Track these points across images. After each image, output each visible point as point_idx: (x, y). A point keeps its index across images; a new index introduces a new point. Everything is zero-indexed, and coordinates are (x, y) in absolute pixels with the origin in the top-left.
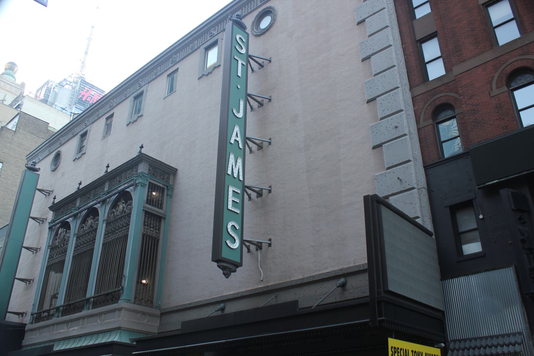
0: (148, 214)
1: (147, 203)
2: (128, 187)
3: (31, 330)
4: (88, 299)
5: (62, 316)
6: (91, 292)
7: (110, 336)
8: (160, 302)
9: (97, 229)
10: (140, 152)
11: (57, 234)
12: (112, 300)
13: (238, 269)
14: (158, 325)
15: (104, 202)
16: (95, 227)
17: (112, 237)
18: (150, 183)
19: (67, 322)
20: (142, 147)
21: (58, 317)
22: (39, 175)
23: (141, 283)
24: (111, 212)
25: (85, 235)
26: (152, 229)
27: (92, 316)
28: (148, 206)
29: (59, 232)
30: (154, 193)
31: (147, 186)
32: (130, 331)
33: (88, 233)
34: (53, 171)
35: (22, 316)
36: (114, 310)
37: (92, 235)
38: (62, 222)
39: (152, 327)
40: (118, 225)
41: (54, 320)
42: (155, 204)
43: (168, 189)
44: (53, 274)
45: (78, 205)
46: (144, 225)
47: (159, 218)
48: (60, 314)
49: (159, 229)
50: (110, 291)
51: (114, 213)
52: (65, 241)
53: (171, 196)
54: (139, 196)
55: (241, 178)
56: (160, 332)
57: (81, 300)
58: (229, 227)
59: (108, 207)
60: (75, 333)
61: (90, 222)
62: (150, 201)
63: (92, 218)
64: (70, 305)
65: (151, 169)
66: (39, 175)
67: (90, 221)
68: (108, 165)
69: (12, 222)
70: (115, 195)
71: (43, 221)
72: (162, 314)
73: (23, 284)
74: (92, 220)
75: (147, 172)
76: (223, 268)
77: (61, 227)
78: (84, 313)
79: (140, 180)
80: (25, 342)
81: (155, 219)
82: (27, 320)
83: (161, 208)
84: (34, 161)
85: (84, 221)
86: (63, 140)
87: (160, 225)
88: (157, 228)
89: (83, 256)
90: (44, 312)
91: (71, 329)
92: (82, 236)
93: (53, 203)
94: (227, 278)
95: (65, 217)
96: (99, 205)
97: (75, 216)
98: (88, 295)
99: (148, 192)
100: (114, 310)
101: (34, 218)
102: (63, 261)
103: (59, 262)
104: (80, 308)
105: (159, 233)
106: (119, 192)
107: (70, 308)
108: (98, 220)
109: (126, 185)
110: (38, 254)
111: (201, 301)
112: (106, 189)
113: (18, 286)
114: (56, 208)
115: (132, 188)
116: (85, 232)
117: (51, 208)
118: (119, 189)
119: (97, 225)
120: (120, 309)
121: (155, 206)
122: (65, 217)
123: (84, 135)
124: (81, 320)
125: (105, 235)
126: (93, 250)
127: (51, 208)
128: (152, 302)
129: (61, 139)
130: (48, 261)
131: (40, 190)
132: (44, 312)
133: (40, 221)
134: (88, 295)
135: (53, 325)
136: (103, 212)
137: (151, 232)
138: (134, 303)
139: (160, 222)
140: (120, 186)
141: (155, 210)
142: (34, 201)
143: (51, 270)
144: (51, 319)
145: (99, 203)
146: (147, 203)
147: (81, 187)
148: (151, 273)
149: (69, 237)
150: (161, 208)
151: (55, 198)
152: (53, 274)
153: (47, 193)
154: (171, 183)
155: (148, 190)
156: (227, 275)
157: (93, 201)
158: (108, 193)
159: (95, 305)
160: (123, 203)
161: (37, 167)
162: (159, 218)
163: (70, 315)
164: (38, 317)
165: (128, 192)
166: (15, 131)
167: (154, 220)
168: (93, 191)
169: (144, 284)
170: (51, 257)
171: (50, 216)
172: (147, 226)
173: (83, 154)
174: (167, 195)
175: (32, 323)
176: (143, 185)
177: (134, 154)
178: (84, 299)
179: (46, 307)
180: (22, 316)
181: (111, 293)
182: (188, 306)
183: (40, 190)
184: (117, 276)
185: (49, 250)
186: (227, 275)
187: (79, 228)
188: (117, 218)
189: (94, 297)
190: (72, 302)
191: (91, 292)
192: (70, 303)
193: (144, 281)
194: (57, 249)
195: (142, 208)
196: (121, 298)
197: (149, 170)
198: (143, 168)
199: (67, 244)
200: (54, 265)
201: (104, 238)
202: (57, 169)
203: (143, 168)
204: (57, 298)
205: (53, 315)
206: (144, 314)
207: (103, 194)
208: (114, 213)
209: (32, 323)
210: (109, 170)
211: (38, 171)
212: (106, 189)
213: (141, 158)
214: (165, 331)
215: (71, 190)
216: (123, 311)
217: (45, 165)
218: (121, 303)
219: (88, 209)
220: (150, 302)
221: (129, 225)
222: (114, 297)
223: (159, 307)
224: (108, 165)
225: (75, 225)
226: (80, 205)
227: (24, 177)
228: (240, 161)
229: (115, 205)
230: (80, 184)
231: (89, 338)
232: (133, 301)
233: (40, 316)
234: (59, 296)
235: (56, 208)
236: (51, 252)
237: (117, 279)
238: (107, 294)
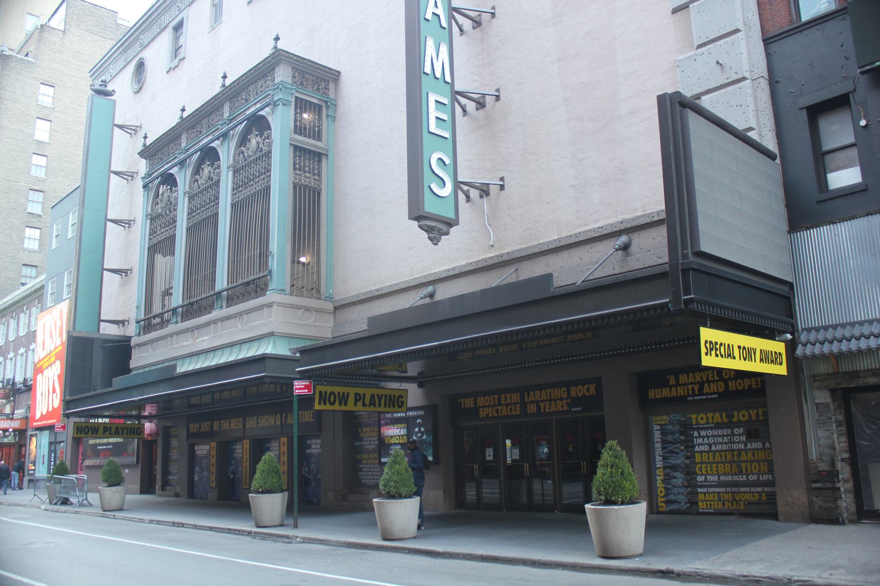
0: (297, 149)
1: (295, 132)
3: (140, 345)
4: (220, 293)
6: (222, 282)
8: (331, 291)
9: (219, 181)
10: (276, 47)
11: (157, 195)
12: (256, 292)
13: (453, 230)
14: (332, 326)
15: (225, 136)
16: (215, 178)
17: (245, 193)
18: (296, 98)
20: (277, 39)
21: (177, 322)
22: (115, 101)
23: (299, 262)
24: (239, 153)
25: (201, 192)
26: (308, 175)
27: (228, 318)
28: (297, 137)
29: (161, 192)
30: (305, 116)
31: (293, 104)
33: (206, 189)
34: (137, 92)
35: (124, 325)
36: (261, 308)
37: (213, 193)
38: (162, 175)
39: (323, 329)
40: (253, 172)
41: (171, 328)
42: (310, 133)
43: (328, 107)
44: (159, 258)
45: (183, 145)
46: (295, 169)
47: (318, 156)
48: (179, 319)
49: (319, 175)
50: (251, 278)
51: (243, 152)
52: (172, 206)
53: (334, 118)
54: (281, 122)
55: (448, 79)
56: (336, 335)
57: (208, 294)
58: (434, 162)
59: (233, 144)
60: (205, 346)
61: (206, 171)
62: (299, 129)
63: (209, 165)
64: (192, 304)
65: (297, 74)
66: (115, 101)
67: (206, 170)
68: (225, 74)
69: (85, 181)
70: (241, 123)
71: (132, 177)
72: (336, 308)
73: (116, 277)
74: (210, 168)
75: (289, 80)
76: (428, 230)
77: (163, 183)
78: (215, 314)
79: (280, 96)
80: (133, 364)
81: (310, 158)
82: (131, 330)
83: (319, 139)
84: (103, 78)
85: (197, 171)
86: (145, 38)
87: (320, 167)
88: (316, 172)
89: (203, 227)
90: (154, 317)
91: (198, 340)
92: (196, 195)
93: (145, 145)
94: (436, 244)
95: (166, 167)
96: (217, 142)
97: (182, 163)
98: (218, 287)
99: (296, 114)
100: (261, 308)
101: (117, 173)
102: (173, 237)
103: (166, 239)
105: (320, 180)
106: (248, 119)
107: (193, 309)
108: (219, 167)
109: (258, 106)
110: (133, 228)
111: (396, 285)
112: (226, 115)
113: (110, 281)
114: (150, 152)
115: (267, 109)
116: (201, 188)
117: (142, 154)
118: (248, 112)
119: (219, 175)
120: (270, 305)
121: (310, 137)
122: (166, 167)
123: (178, 27)
126: (216, 215)
127: (142, 154)
128: (319, 291)
129: (142, 37)
130: (150, 239)
131: (120, 127)
132: (154, 317)
133: (127, 176)
134: (218, 287)
136: (227, 153)
137: (307, 180)
138: (291, 294)
139: (320, 161)
140: (249, 108)
141: (309, 143)
142: (114, 145)
143: (155, 252)
144: (167, 326)
145: (218, 139)
146: (295, 132)
147: (185, 114)
148: (313, 245)
149: (176, 198)
150: (319, 139)
151: (145, 137)
152: (159, 258)
153: (131, 130)
154: (332, 96)
155: (295, 110)
156: (435, 241)
158: (231, 121)
159: (231, 300)
160: (257, 135)
161: (110, 88)
162: (318, 156)
164: (147, 326)
165: (263, 117)
166: (64, 32)
167: (309, 160)
168: (206, 120)
169: (303, 264)
170: (152, 233)
171: (142, 166)
172: (300, 170)
173: (181, 60)
174: (328, 116)
175: (139, 335)
176: (286, 104)
177: (266, 51)
178: (212, 293)
179: (157, 309)
180: (124, 325)
181: (253, 280)
182: (377, 294)
183: (120, 127)
184: (260, 254)
185: (149, 221)
186: (435, 241)
187: (190, 182)
188: (249, 160)
189: (227, 290)
190: (195, 299)
191: (222, 282)
192: (192, 300)
193: (303, 260)
194: (160, 220)
195: (288, 142)
196: (270, 288)
197: (294, 77)
198: (283, 74)
199: (175, 210)
200: (160, 246)
201: (233, 195)
202: (143, 90)
203: (283, 74)
204: (171, 294)
205: (168, 321)
206: (308, 309)
207: (223, 124)
208: (243, 152)
209: (139, 335)
210: (228, 82)
211: (111, 95)
212: (226, 115)
213: (278, 57)
214: (344, 333)
215: (172, 121)
216: (275, 307)
217: (122, 84)
218: (271, 296)
219: (201, 150)
220: (315, 291)
221: (270, 170)
222: (257, 287)
223: (329, 298)
224: (225, 74)
225: (183, 178)
227: (91, 107)
228: (444, 49)
229: (243, 141)
230: (183, 110)
231: (227, 351)
232: (288, 291)
233: (149, 324)
234: (173, 291)
235: (150, 152)
236: (151, 224)
237: (260, 258)
238: (248, 283)
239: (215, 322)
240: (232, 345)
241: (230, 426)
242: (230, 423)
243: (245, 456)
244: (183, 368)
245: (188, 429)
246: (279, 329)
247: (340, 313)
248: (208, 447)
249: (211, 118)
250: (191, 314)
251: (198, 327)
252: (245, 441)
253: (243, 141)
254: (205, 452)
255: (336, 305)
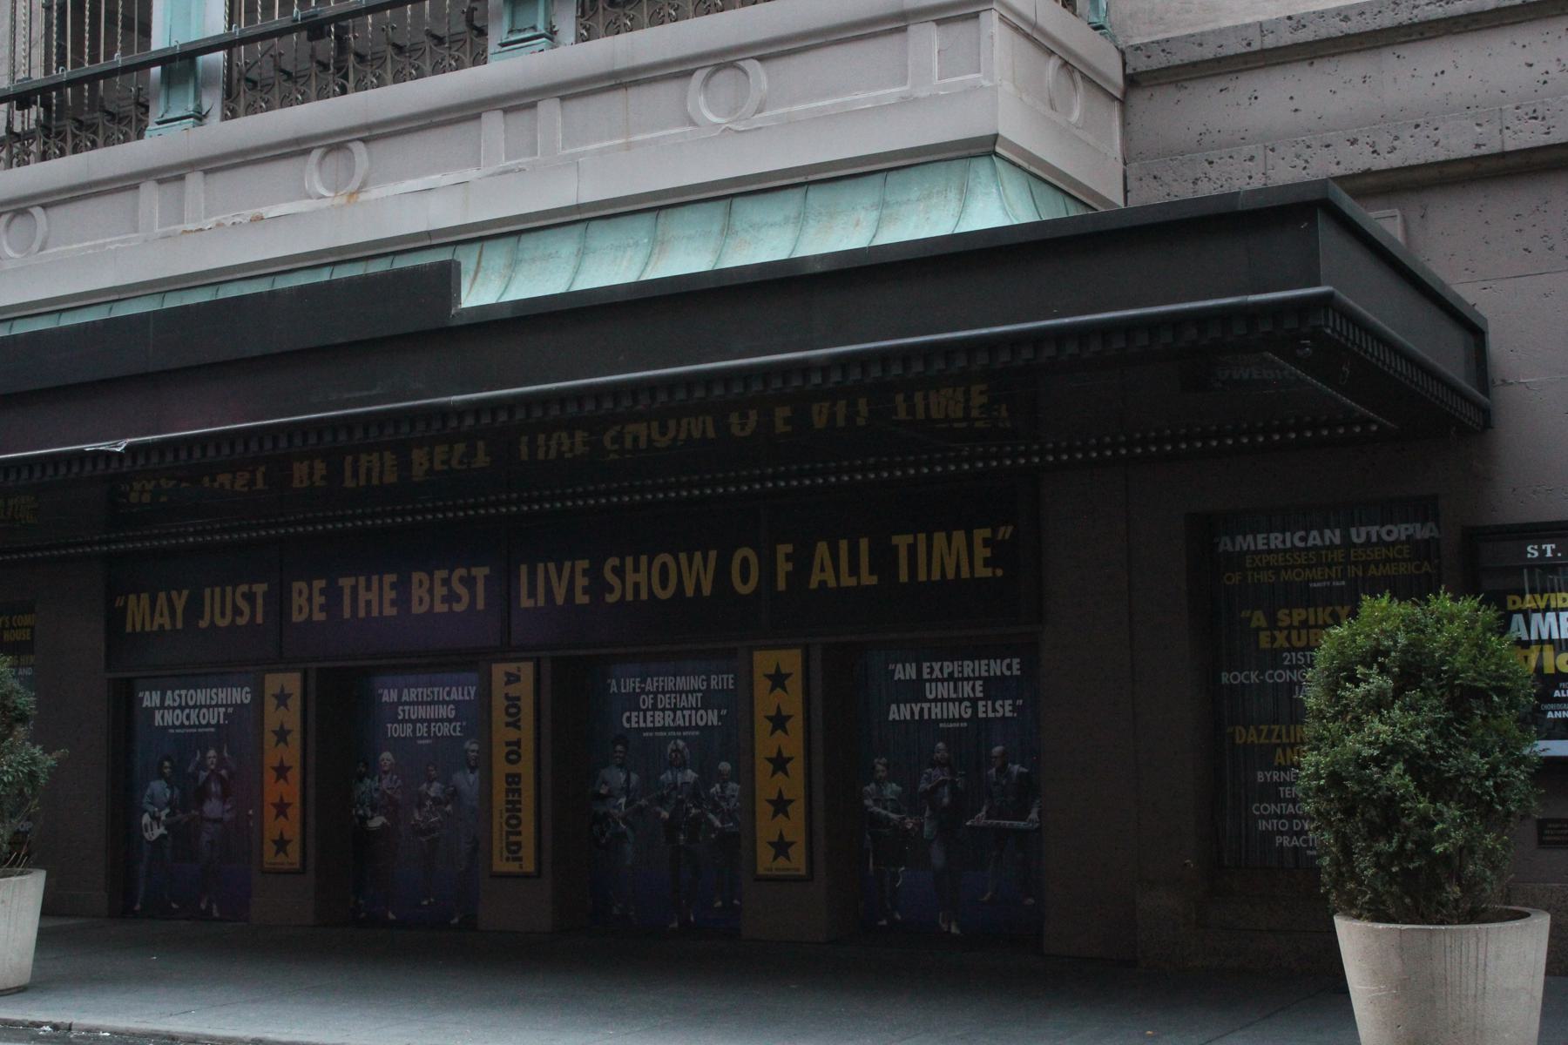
5: (230, 113)
7: (884, 204)
19: (335, 143)
21: (200, 117)
32: (1038, 176)
48: (212, 101)
72: (1133, 81)
78: (503, 69)
91: (374, 193)
104: (128, 121)
124: (493, 122)
135: (170, 175)
163: (354, 98)
239: (516, 103)
240: (656, 207)
241: (403, 601)
242: (403, 587)
243: (502, 734)
244: (482, 290)
245: (115, 619)
246: (1017, 126)
247: (1139, 99)
248: (240, 696)
250: (92, 128)
251: (374, 133)
252: (499, 671)
254: (213, 717)
255: (1140, 64)
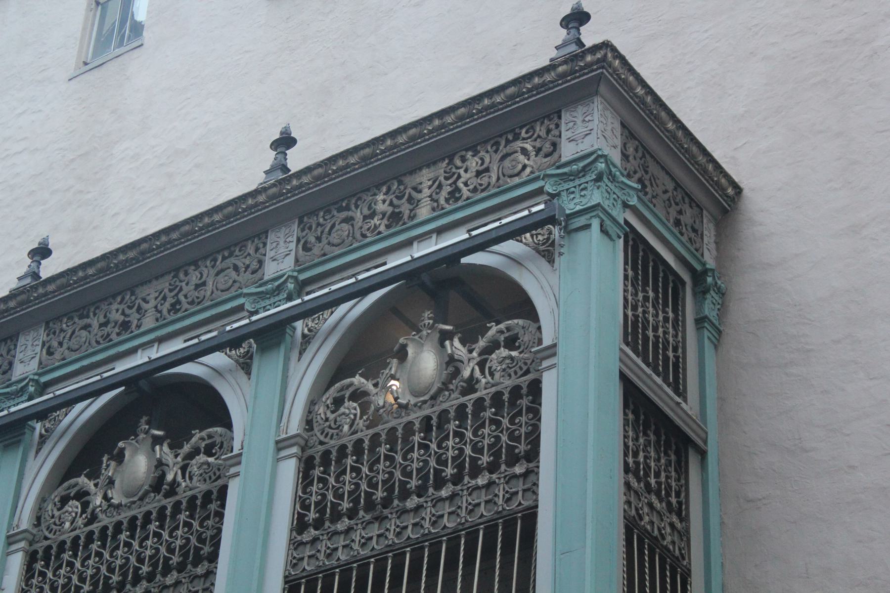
2: (483, 245)
15: (271, 335)
43: (701, 291)
49: (681, 511)
53: (714, 329)
59: (306, 371)
70: (363, 293)
79: (595, 197)
96: (218, 359)
109: (177, 345)
125: (300, 525)
139: (682, 469)
145: (232, 343)
157: (161, 340)
158: (302, 286)
168: (164, 284)
174: (700, 321)
177: (535, 47)
198: (592, 131)
207: (262, 296)
226: (43, 368)
229: (365, 352)
230: (42, 252)
249: (194, 277)
253: (93, 451)
